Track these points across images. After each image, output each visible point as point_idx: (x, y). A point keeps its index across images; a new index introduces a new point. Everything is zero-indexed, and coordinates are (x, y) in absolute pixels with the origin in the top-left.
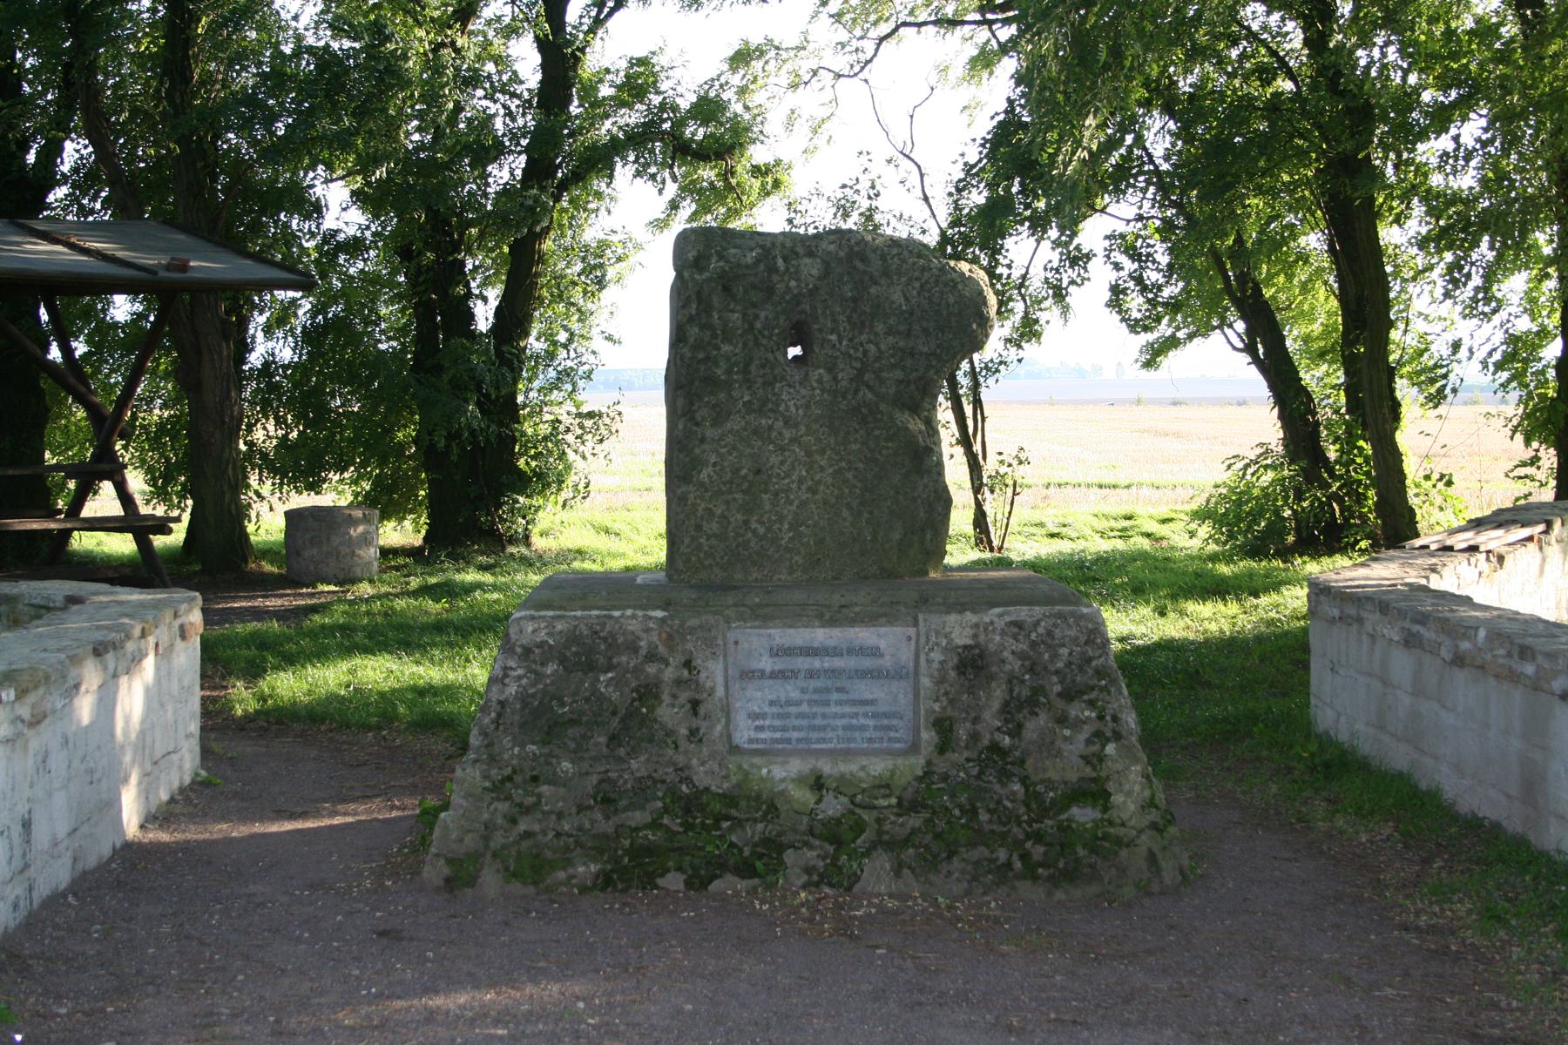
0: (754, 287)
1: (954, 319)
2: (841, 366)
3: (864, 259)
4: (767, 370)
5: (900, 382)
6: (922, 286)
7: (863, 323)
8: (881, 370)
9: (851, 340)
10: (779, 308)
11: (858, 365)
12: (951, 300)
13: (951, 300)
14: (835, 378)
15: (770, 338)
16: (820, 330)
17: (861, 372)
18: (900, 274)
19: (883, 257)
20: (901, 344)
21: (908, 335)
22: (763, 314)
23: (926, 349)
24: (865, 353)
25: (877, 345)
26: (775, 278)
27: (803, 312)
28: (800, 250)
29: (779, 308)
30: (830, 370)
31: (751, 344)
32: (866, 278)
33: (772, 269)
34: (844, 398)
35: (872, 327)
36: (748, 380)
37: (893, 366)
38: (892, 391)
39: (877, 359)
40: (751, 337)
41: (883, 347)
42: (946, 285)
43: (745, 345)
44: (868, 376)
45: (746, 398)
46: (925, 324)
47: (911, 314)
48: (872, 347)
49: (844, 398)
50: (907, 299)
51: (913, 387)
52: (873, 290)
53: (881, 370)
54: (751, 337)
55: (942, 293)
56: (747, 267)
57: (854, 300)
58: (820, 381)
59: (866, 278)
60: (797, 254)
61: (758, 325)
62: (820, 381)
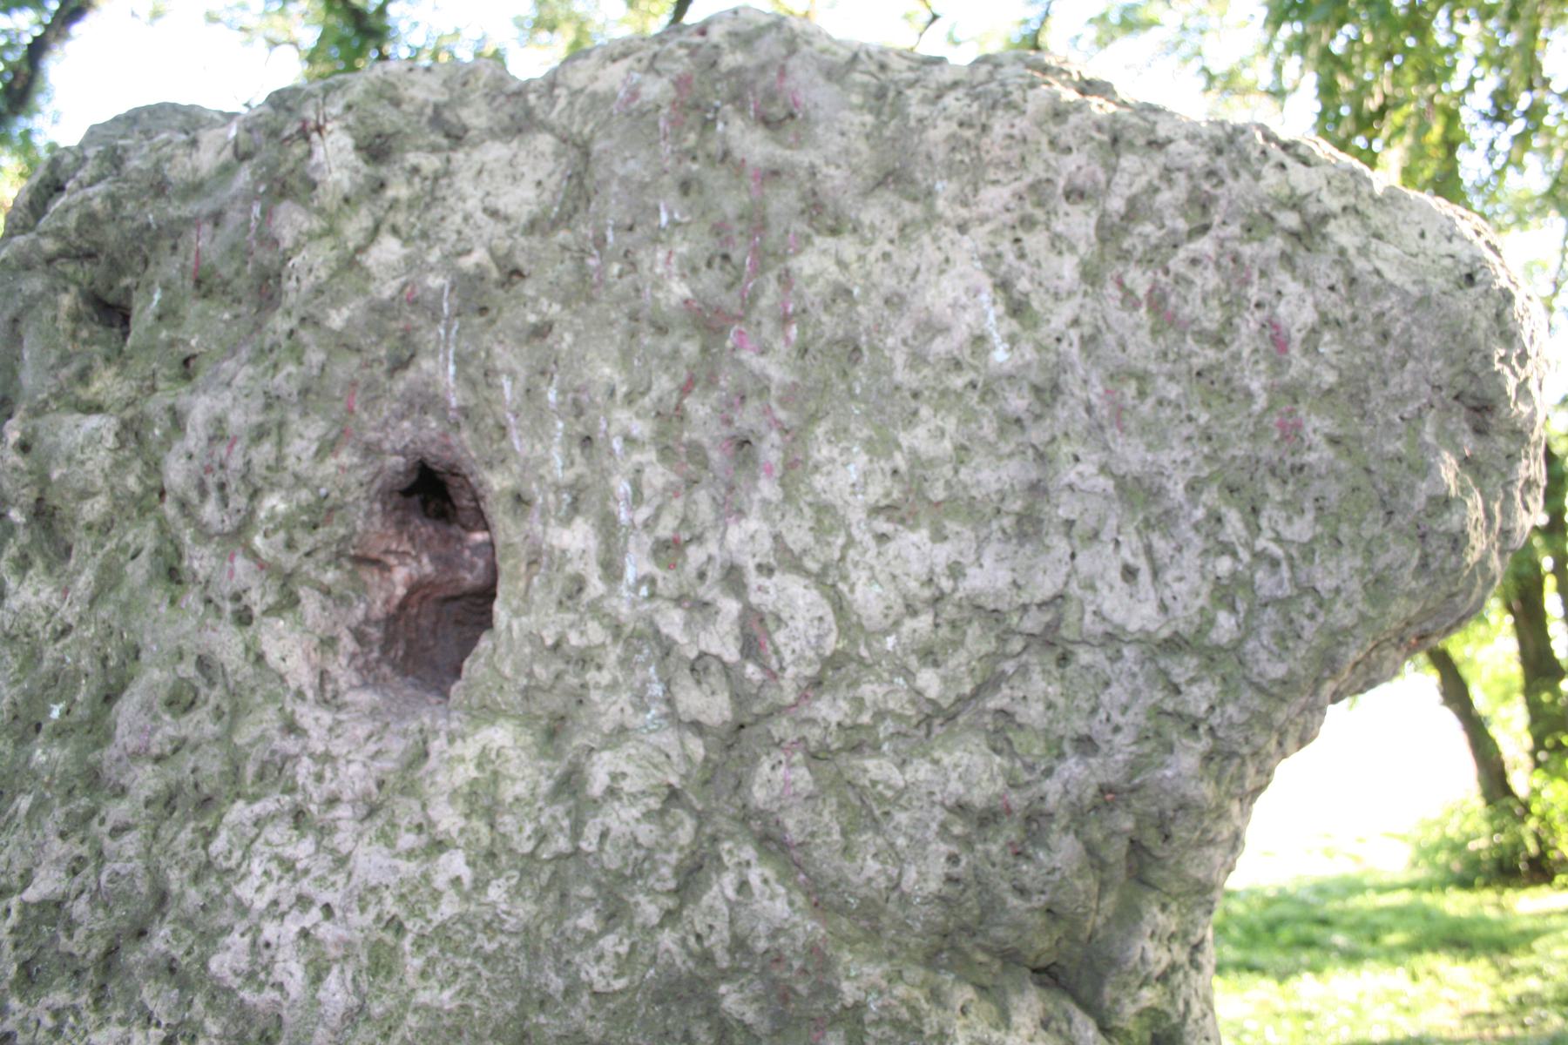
0: (204, 284)
1: (1316, 425)
2: (612, 709)
3: (779, 119)
4: (201, 724)
5: (987, 819)
6: (1108, 232)
7: (743, 444)
8: (858, 741)
9: (668, 551)
10: (287, 378)
11: (713, 706)
12: (1297, 312)
13: (1297, 312)
14: (570, 784)
15: (239, 535)
16: (520, 500)
17: (737, 740)
18: (974, 174)
19: (884, 98)
20: (988, 577)
21: (1028, 527)
22: (201, 408)
23: (1138, 613)
24: (754, 634)
25: (828, 582)
26: (291, 221)
27: (424, 402)
28: (475, 116)
29: (287, 378)
30: (553, 732)
31: (137, 572)
32: (781, 202)
33: (288, 186)
34: (615, 914)
35: (795, 469)
36: (93, 779)
37: (936, 719)
38: (926, 876)
39: (831, 672)
40: (144, 536)
41: (868, 597)
42: (1257, 224)
43: (109, 579)
44: (775, 780)
45: (46, 884)
46: (1133, 455)
47: (1048, 393)
48: (796, 601)
49: (615, 914)
50: (1018, 309)
51: (1064, 850)
52: (816, 262)
53: (858, 741)
54: (144, 536)
55: (1235, 268)
56: (195, 189)
57: (708, 322)
58: (481, 800)
59: (781, 202)
60: (457, 137)
61: (176, 473)
62: (481, 800)
